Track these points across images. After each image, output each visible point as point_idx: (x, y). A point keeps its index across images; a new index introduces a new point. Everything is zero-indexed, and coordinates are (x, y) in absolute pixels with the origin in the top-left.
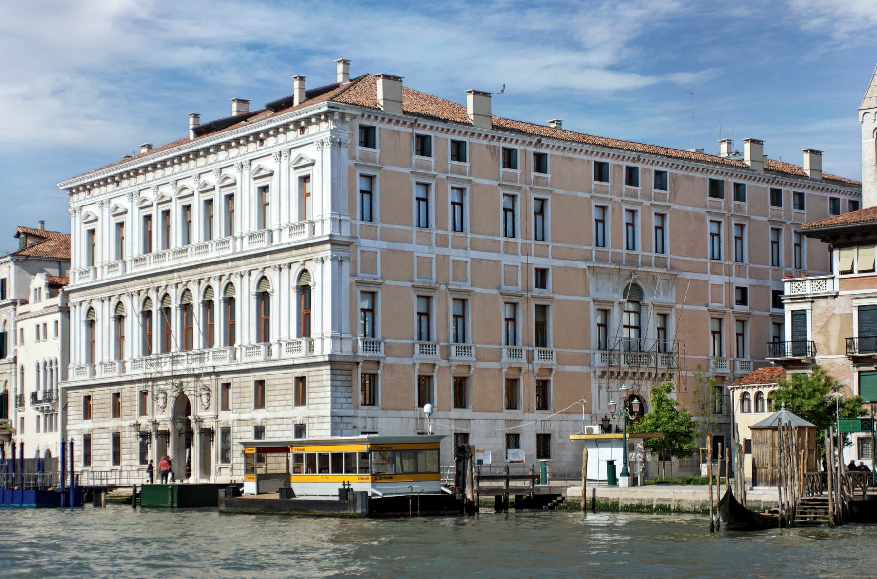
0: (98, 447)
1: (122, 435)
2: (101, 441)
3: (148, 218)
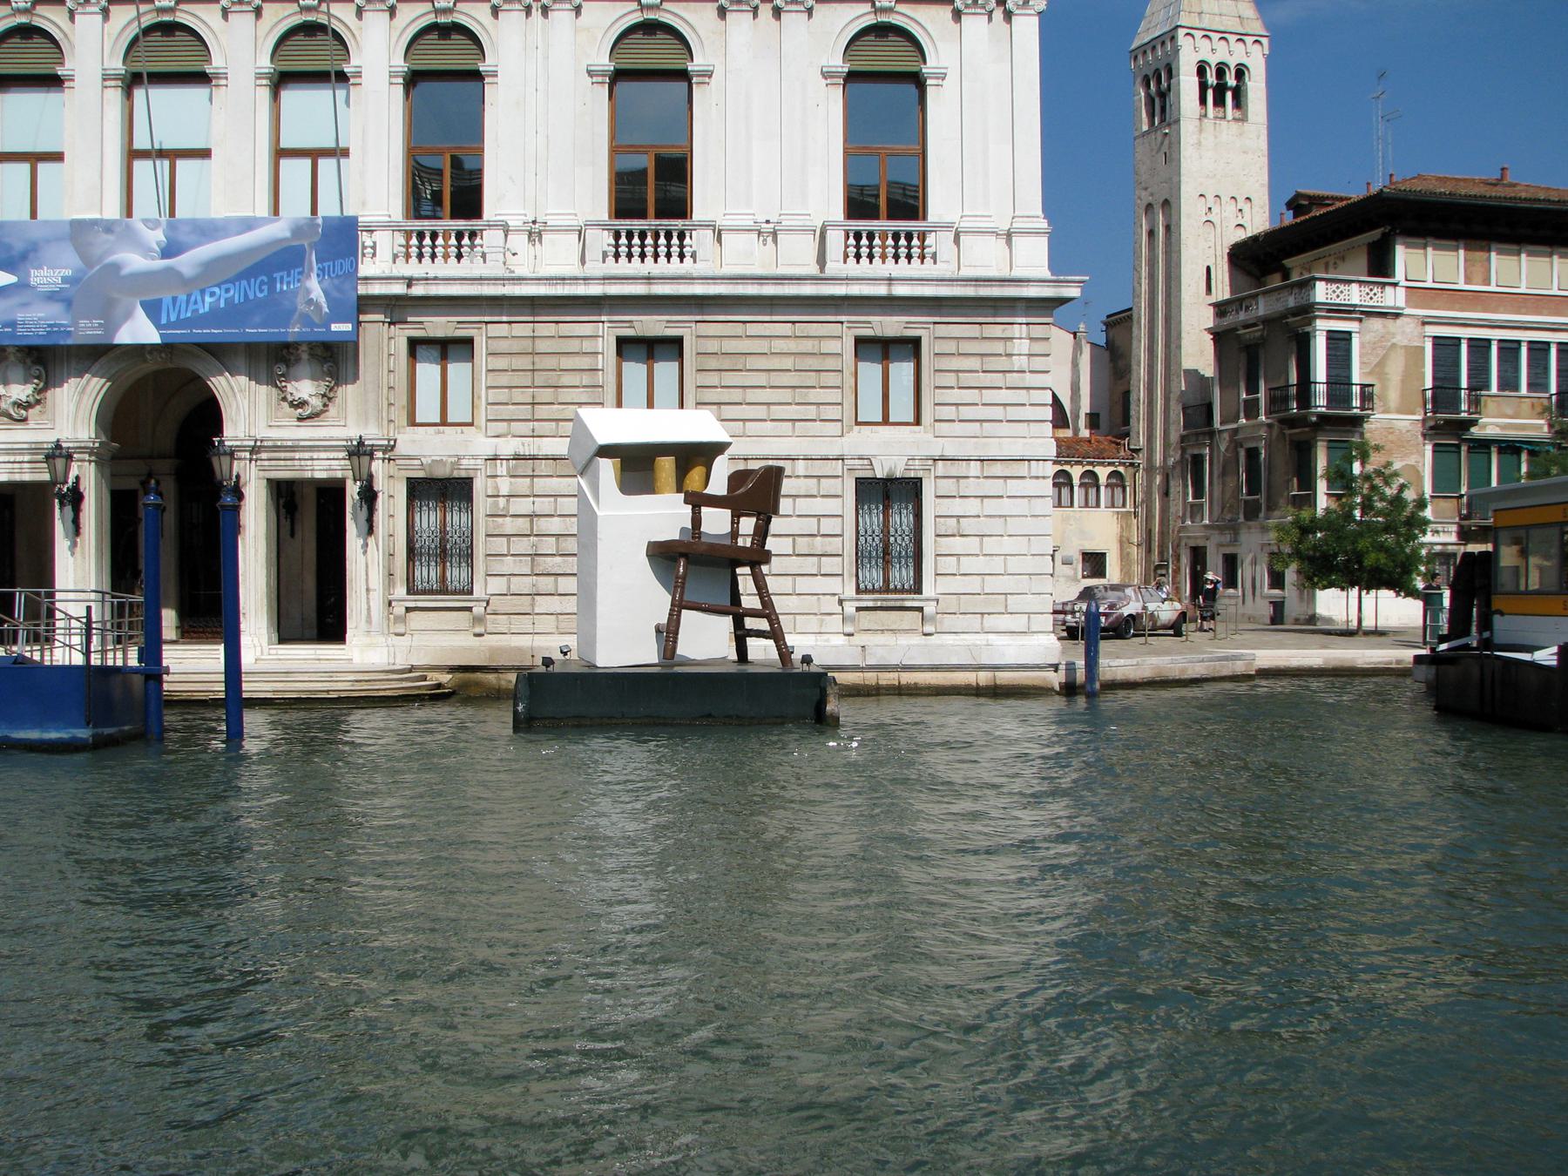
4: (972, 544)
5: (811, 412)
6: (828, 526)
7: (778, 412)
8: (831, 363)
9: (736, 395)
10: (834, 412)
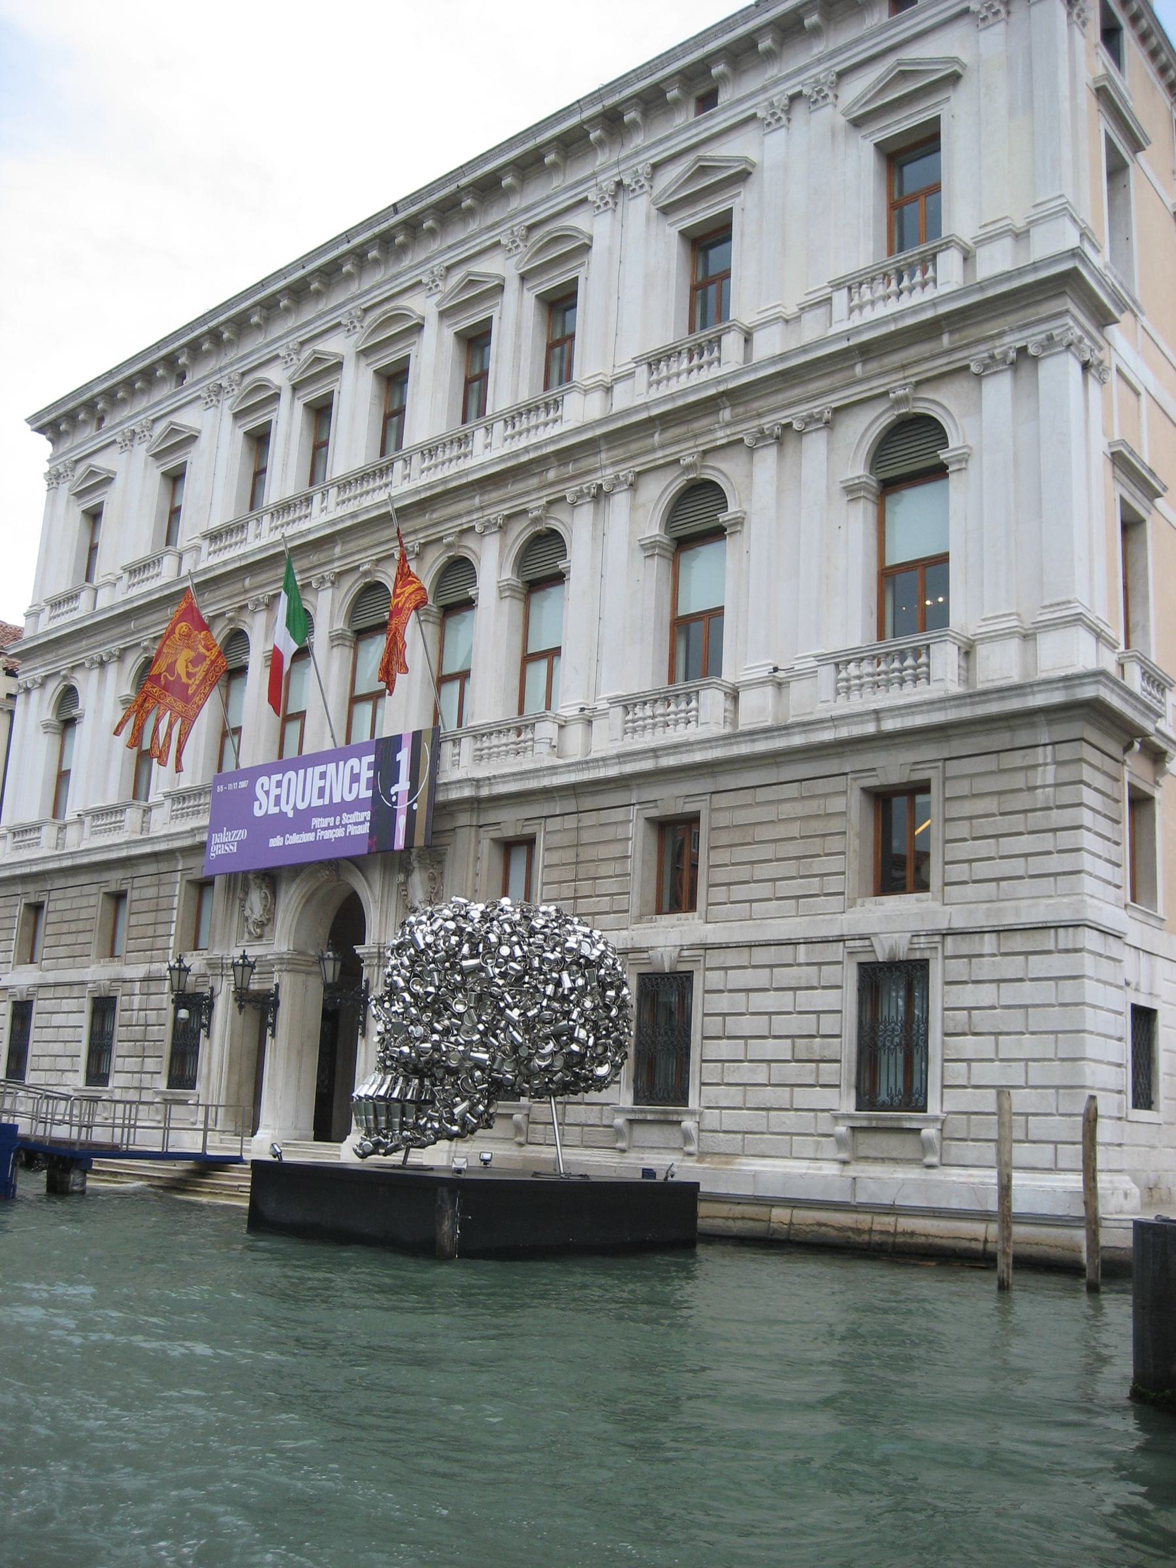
0: (48, 1034)
1: (122, 1002)
2: (57, 1020)
3: (259, 439)
4: (985, 1046)
5: (814, 885)
6: (829, 1024)
7: (785, 888)
8: (835, 825)
9: (743, 873)
10: (834, 884)
